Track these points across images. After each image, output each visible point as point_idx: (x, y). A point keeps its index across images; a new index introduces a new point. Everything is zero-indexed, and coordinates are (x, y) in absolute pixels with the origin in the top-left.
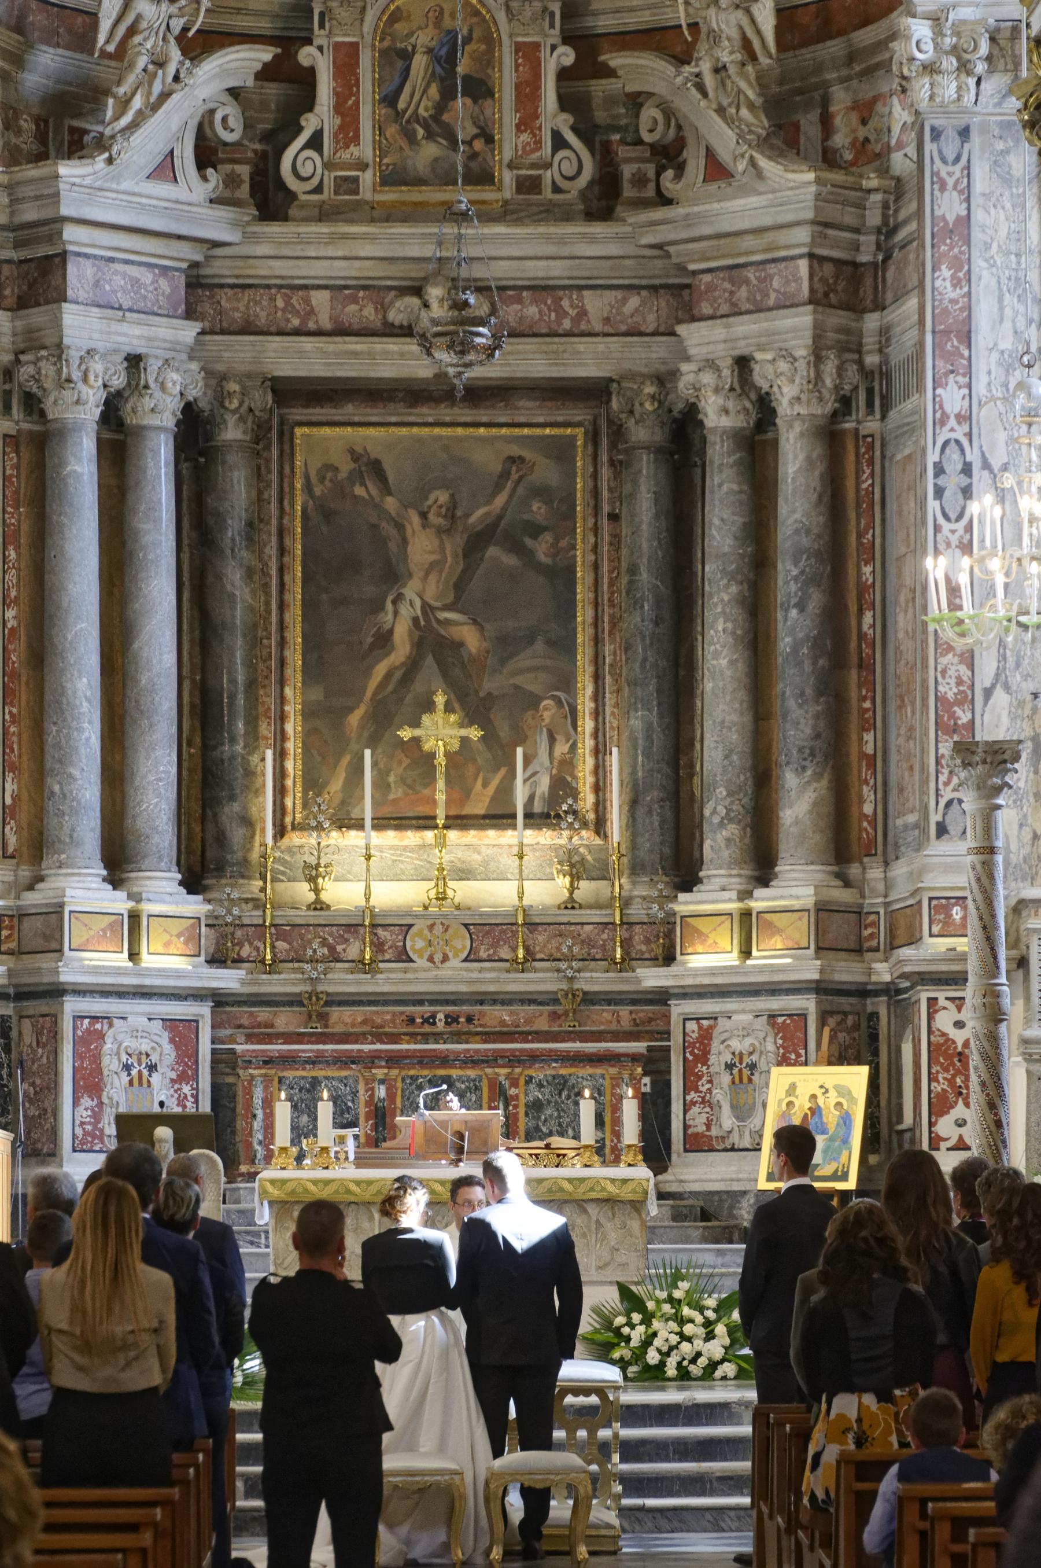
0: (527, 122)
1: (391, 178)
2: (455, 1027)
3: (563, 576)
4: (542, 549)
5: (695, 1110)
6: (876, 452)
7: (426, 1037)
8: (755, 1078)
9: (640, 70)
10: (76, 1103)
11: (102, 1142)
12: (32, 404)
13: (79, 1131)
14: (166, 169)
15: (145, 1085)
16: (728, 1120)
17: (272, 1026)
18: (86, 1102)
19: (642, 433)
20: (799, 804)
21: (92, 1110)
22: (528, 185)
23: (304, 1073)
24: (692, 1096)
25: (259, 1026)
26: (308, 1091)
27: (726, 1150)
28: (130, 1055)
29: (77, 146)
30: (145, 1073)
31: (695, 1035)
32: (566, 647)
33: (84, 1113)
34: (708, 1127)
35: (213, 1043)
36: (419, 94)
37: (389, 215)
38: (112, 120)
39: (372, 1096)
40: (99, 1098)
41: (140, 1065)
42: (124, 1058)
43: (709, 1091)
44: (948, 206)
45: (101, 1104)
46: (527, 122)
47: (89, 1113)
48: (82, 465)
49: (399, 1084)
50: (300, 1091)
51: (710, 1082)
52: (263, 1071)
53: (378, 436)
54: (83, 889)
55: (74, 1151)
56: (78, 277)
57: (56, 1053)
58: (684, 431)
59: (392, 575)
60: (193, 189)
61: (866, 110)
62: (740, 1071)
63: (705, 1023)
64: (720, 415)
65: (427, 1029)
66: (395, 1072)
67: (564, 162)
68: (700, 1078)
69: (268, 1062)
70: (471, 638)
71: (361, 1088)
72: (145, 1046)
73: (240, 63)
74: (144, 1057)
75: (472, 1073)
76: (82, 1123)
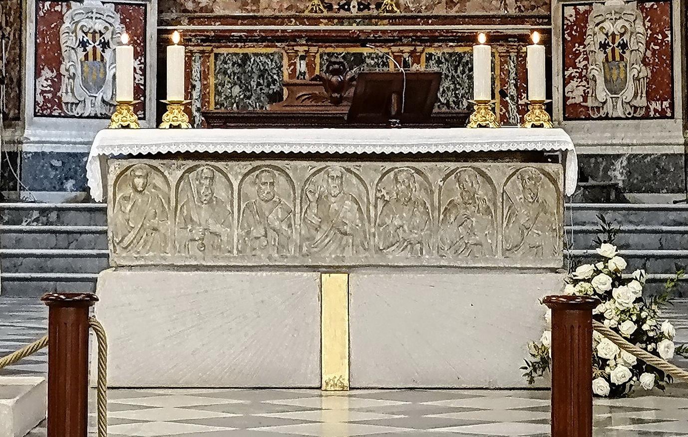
2: (366, 13)
5: (574, 83)
7: (341, 21)
8: (626, 56)
10: (37, 74)
11: (61, 109)
13: (40, 99)
15: (99, 59)
16: (602, 93)
17: (212, 11)
18: (47, 73)
21: (52, 81)
23: (237, 50)
24: (571, 71)
25: (201, 10)
26: (239, 65)
27: (600, 118)
28: (86, 34)
30: (99, 49)
31: (573, 19)
33: (43, 83)
34: (585, 99)
35: (158, 26)
39: (294, 70)
40: (58, 70)
41: (94, 42)
42: (80, 35)
43: (586, 67)
45: (59, 75)
47: (49, 83)
49: (318, 61)
50: (233, 65)
51: (587, 59)
52: (201, 48)
55: (35, 115)
57: (20, 31)
62: (613, 50)
63: (582, 8)
65: (342, 13)
66: (313, 49)
68: (577, 55)
69: (207, 39)
71: (285, 62)
72: (99, 26)
74: (97, 35)
75: (381, 51)
76: (43, 92)
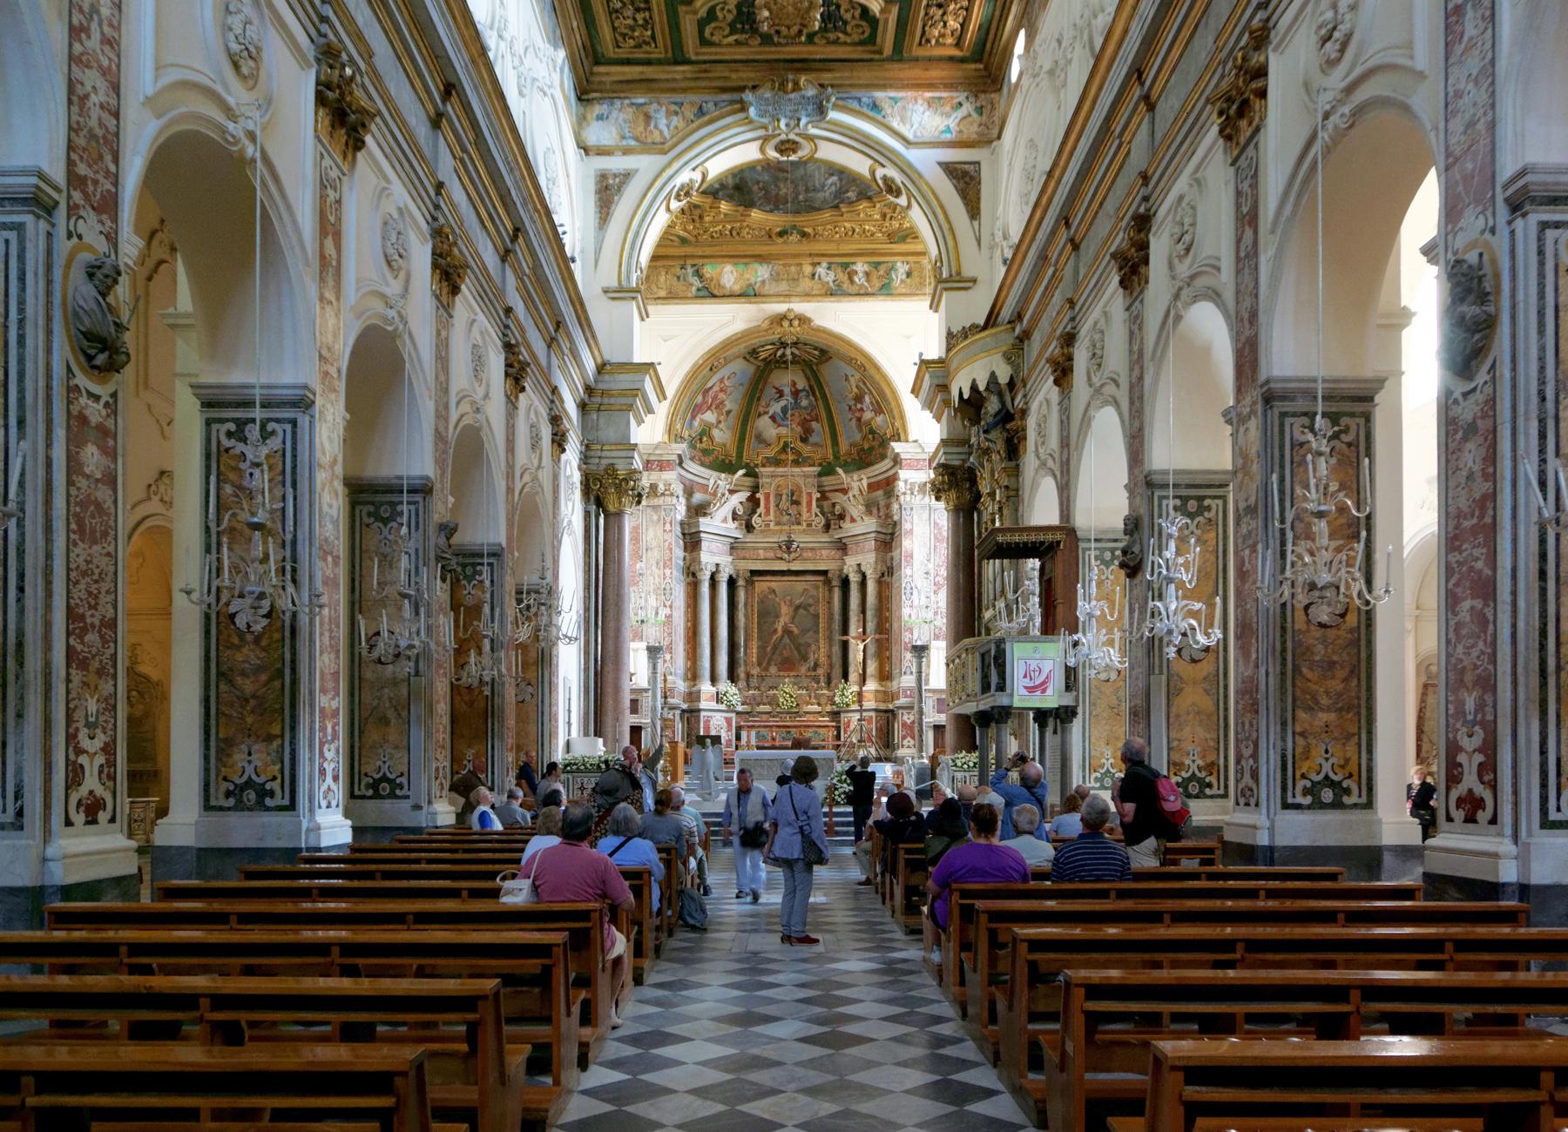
0: (809, 510)
1: (778, 523)
3: (817, 616)
4: (812, 609)
6: (889, 586)
9: (838, 497)
12: (694, 575)
14: (725, 520)
19: (835, 583)
20: (872, 667)
22: (809, 525)
29: (705, 514)
32: (817, 632)
36: (784, 504)
37: (774, 533)
38: (712, 509)
44: (906, 526)
46: (809, 510)
48: (705, 589)
53: (775, 584)
54: (706, 687)
56: (704, 545)
58: (845, 583)
59: (777, 616)
60: (732, 525)
61: (888, 506)
64: (854, 578)
67: (817, 520)
70: (796, 631)
73: (743, 496)
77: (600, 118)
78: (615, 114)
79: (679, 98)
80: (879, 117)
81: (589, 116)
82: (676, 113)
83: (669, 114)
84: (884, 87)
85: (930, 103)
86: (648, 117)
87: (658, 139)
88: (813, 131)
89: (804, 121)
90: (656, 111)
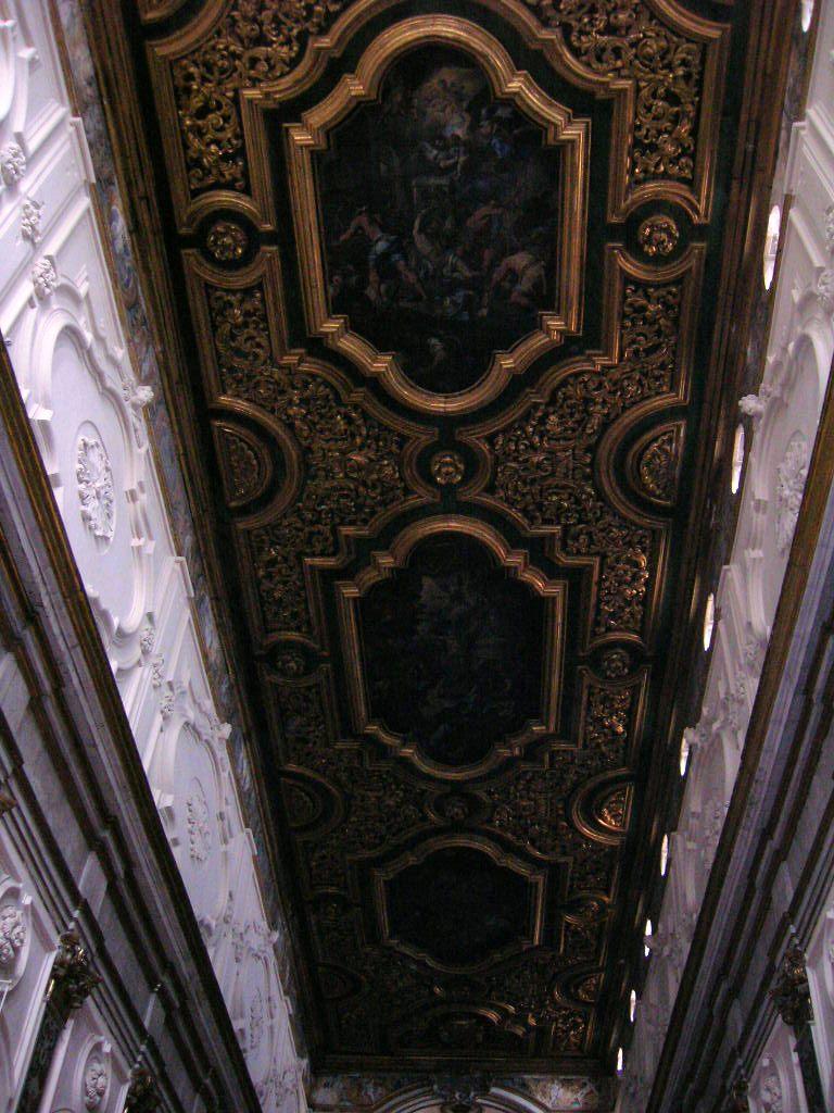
77: (326, 1085)
78: (337, 1084)
79: (382, 1075)
80: (526, 1092)
81: (319, 1085)
82: (381, 1085)
83: (375, 1084)
84: (526, 1072)
85: (566, 1083)
86: (360, 1087)
87: (367, 1101)
88: (479, 1101)
89: (472, 1094)
90: (367, 1083)
